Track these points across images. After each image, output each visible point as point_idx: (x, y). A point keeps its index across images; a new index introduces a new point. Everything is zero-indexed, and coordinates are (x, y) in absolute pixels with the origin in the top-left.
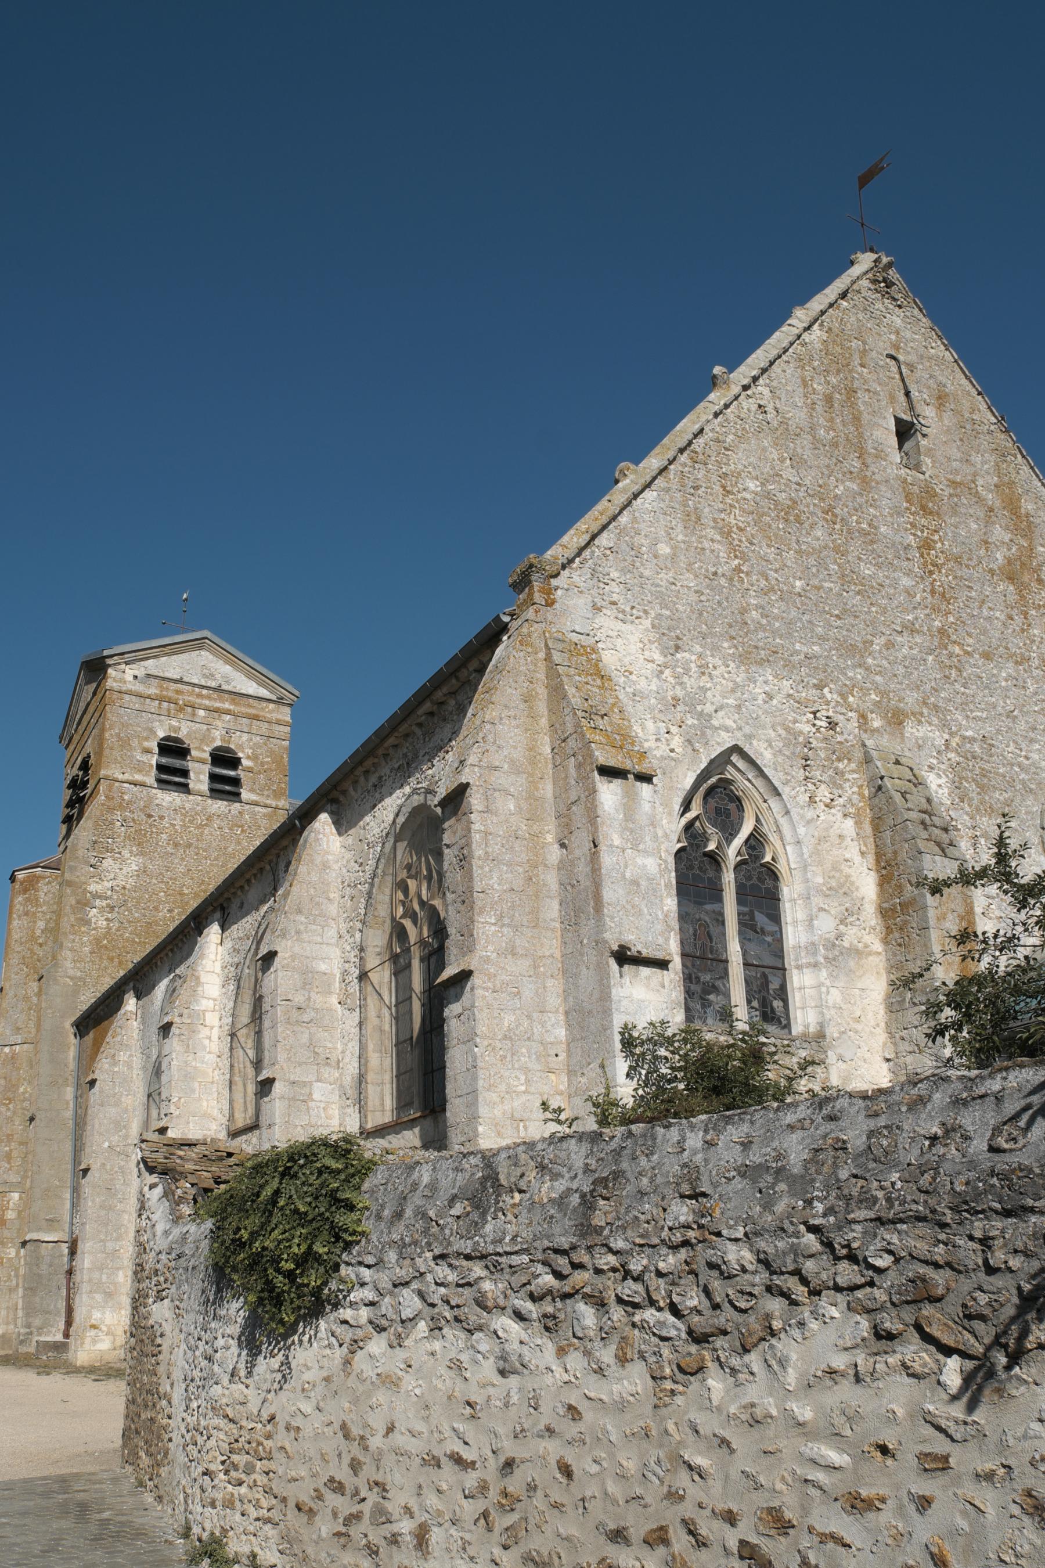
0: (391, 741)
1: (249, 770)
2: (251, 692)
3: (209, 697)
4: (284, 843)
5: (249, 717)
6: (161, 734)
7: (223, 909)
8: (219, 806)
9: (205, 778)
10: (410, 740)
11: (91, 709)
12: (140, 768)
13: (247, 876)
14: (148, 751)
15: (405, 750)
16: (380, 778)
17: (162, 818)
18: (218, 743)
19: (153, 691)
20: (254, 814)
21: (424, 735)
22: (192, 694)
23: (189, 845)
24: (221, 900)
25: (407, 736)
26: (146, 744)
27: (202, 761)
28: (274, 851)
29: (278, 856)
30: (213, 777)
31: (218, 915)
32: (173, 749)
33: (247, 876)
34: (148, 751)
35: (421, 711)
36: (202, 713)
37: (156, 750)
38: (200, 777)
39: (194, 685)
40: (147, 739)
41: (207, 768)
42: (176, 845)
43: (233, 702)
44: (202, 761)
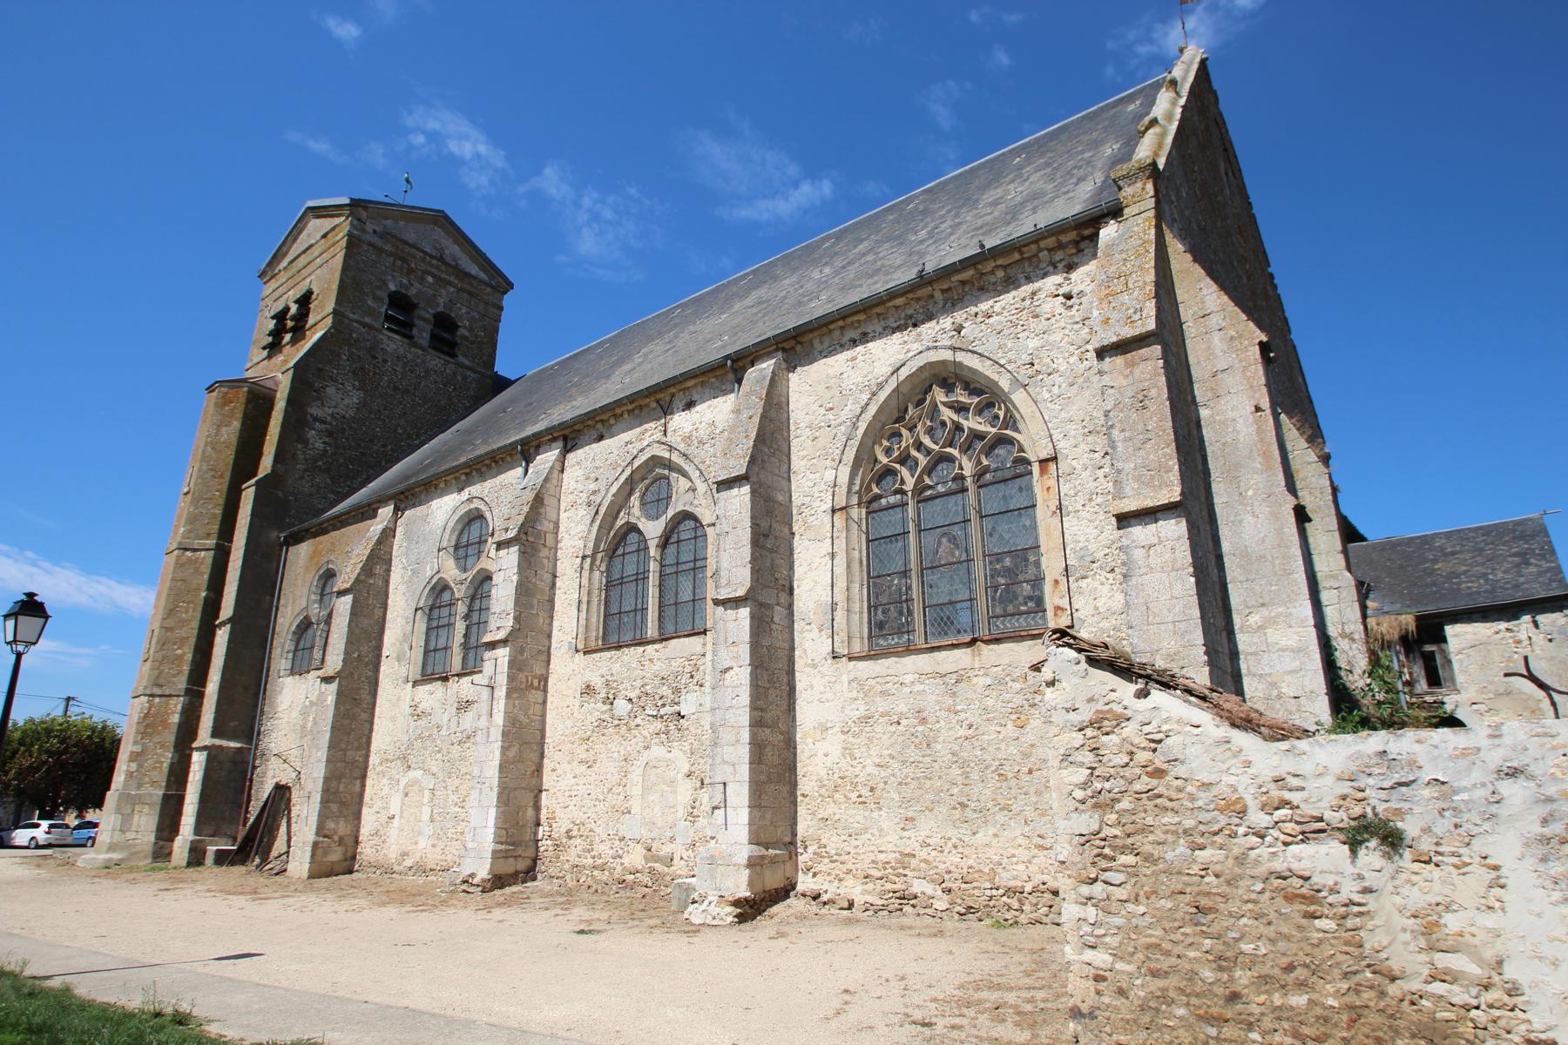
0: (899, 301)
1: (464, 338)
2: (473, 272)
3: (438, 268)
4: (690, 383)
5: (471, 294)
6: (392, 287)
7: (565, 438)
8: (435, 361)
9: (426, 335)
10: (922, 303)
11: (316, 251)
12: (371, 312)
13: (618, 411)
14: (380, 300)
15: (910, 312)
16: (865, 334)
17: (385, 361)
18: (441, 309)
19: (388, 247)
20: (465, 377)
21: (946, 301)
22: (423, 260)
23: (406, 391)
24: (566, 432)
25: (918, 299)
26: (378, 293)
27: (424, 319)
28: (672, 390)
29: (673, 395)
30: (434, 337)
31: (560, 444)
32: (401, 304)
33: (618, 411)
34: (380, 300)
35: (956, 278)
36: (430, 279)
37: (387, 300)
38: (423, 333)
39: (426, 253)
40: (379, 288)
41: (429, 327)
42: (396, 388)
43: (457, 277)
44: (424, 319)
